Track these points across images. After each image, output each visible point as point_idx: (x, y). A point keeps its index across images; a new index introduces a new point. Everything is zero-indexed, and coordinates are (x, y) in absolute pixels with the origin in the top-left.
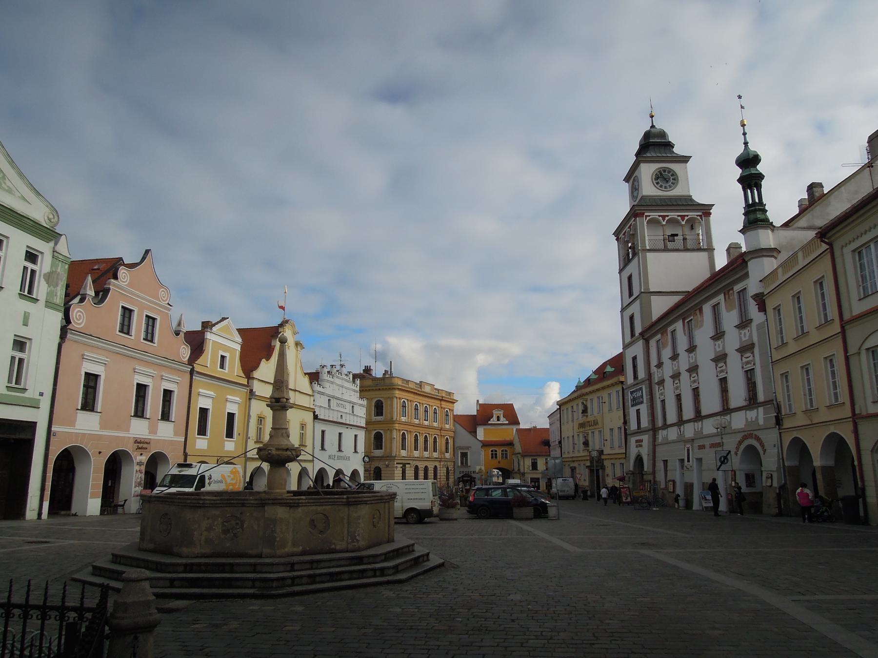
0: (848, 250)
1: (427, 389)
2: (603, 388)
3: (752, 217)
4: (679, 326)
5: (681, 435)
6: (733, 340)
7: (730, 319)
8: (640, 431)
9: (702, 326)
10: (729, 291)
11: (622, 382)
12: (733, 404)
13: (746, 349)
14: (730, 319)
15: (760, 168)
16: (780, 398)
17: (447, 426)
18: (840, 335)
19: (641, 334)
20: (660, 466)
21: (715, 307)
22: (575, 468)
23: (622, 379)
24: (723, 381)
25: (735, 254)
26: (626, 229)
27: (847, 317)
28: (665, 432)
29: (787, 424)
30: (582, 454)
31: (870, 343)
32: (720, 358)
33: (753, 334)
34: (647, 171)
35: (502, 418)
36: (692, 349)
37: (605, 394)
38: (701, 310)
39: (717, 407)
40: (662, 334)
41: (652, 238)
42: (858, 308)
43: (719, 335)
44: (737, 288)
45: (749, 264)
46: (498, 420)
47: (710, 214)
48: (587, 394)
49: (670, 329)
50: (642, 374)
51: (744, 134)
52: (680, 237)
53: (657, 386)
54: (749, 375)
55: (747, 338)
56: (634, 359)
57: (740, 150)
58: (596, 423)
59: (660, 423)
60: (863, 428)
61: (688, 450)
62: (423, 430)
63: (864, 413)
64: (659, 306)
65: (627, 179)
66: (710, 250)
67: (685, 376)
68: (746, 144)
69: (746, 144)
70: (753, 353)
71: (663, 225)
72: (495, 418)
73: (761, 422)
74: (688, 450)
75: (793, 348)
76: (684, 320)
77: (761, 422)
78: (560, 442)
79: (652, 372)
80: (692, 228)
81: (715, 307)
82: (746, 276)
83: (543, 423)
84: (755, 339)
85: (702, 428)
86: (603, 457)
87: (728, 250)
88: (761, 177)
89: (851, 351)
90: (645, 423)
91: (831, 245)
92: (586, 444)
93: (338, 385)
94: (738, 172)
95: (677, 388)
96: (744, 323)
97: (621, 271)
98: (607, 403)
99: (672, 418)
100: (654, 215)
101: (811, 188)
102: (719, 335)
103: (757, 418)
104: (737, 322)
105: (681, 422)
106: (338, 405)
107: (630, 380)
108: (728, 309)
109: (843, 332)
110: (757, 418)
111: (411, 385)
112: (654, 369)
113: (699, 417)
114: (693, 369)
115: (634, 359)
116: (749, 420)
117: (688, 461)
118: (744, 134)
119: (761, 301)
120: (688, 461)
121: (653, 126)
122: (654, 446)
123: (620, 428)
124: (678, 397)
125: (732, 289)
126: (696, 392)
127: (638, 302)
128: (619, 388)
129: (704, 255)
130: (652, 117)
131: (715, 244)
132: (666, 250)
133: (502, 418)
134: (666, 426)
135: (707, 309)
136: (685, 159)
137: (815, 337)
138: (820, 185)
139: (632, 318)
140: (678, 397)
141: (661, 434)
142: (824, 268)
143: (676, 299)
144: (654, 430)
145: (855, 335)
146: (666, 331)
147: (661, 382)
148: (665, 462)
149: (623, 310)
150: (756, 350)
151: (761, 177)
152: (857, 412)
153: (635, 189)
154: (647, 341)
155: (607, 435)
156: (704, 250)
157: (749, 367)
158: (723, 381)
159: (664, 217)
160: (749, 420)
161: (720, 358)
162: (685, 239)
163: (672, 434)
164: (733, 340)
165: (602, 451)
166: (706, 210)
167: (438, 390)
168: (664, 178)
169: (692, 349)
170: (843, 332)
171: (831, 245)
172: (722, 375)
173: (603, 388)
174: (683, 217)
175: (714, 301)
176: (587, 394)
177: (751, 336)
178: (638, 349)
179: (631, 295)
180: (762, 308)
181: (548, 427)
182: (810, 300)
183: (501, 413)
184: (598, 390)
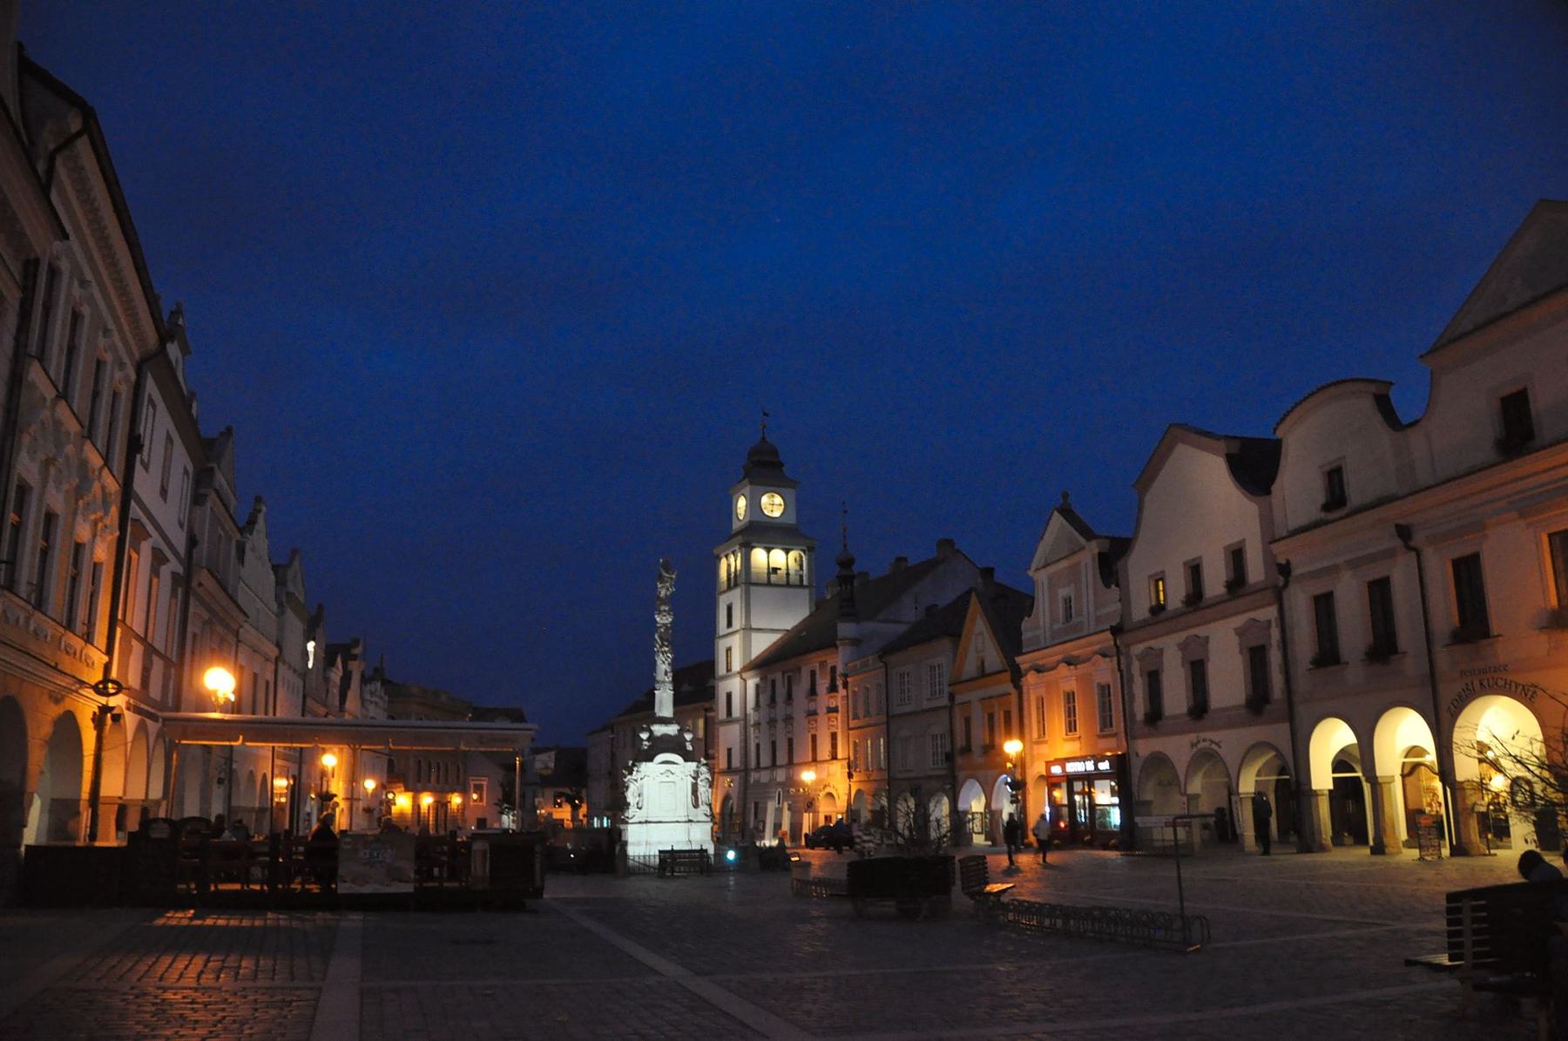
4: (778, 676)
5: (773, 780)
7: (823, 684)
8: (730, 770)
14: (823, 684)
19: (740, 673)
21: (813, 674)
23: (707, 705)
42: (897, 710)
49: (770, 677)
50: (736, 712)
59: (753, 764)
67: (780, 725)
81: (813, 674)
90: (736, 763)
99: (765, 760)
105: (774, 765)
107: (722, 714)
112: (750, 710)
114: (789, 719)
124: (774, 744)
126: (790, 741)
132: (769, 584)
134: (758, 768)
140: (774, 744)
141: (753, 776)
143: (775, 637)
144: (745, 771)
148: (756, 804)
163: (764, 777)
179: (730, 624)
180: (845, 686)
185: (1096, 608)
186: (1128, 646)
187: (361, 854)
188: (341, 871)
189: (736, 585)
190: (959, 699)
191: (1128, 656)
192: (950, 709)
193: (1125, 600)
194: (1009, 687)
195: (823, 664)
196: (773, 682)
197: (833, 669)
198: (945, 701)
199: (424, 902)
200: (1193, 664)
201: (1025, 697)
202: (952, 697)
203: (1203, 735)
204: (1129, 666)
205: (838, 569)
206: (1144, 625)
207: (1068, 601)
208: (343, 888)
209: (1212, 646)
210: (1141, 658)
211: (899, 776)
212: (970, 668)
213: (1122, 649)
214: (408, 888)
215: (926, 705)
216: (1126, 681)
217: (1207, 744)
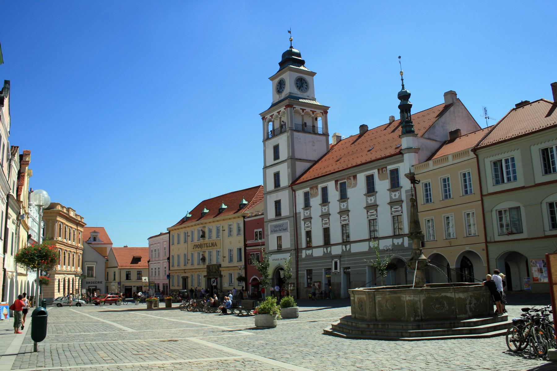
1: (72, 214)
7: (382, 185)
9: (355, 185)
10: (382, 169)
12: (380, 234)
14: (382, 185)
15: (411, 101)
17: (80, 245)
18: (480, 202)
20: (303, 273)
22: (187, 277)
26: (275, 113)
27: (485, 193)
28: (309, 252)
29: (427, 245)
30: (196, 266)
34: (289, 77)
38: (355, 177)
40: (311, 188)
45: (405, 155)
47: (327, 112)
48: (206, 223)
51: (402, 80)
53: (302, 222)
55: (397, 197)
56: (278, 204)
57: (400, 89)
58: (213, 245)
59: (304, 245)
60: (491, 247)
61: (336, 263)
62: (69, 249)
63: (493, 240)
65: (272, 78)
66: (326, 134)
68: (403, 85)
69: (403, 85)
70: (401, 206)
71: (302, 116)
73: (406, 244)
74: (336, 263)
76: (336, 182)
77: (406, 244)
78: (169, 259)
79: (298, 211)
82: (402, 161)
83: (146, 245)
85: (350, 249)
86: (221, 269)
88: (410, 106)
92: (203, 259)
94: (399, 102)
95: (326, 224)
97: (264, 141)
103: (403, 243)
108: (380, 179)
110: (403, 243)
111: (65, 210)
113: (346, 241)
114: (344, 212)
115: (278, 204)
116: (396, 244)
117: (336, 268)
118: (402, 80)
120: (336, 268)
121: (291, 47)
122: (297, 262)
123: (240, 249)
125: (386, 168)
127: (285, 165)
130: (291, 41)
136: (313, 74)
139: (277, 176)
147: (308, 219)
149: (265, 168)
150: (404, 205)
151: (410, 106)
152: (488, 240)
153: (280, 87)
154: (294, 191)
155: (227, 254)
159: (303, 110)
160: (396, 244)
165: (220, 265)
166: (325, 110)
167: (76, 215)
168: (302, 83)
170: (482, 200)
176: (206, 223)
177: (400, 196)
178: (284, 197)
181: (147, 246)
189: (281, 132)
195: (381, 170)
196: (325, 190)
205: (400, 101)
211: (497, 238)
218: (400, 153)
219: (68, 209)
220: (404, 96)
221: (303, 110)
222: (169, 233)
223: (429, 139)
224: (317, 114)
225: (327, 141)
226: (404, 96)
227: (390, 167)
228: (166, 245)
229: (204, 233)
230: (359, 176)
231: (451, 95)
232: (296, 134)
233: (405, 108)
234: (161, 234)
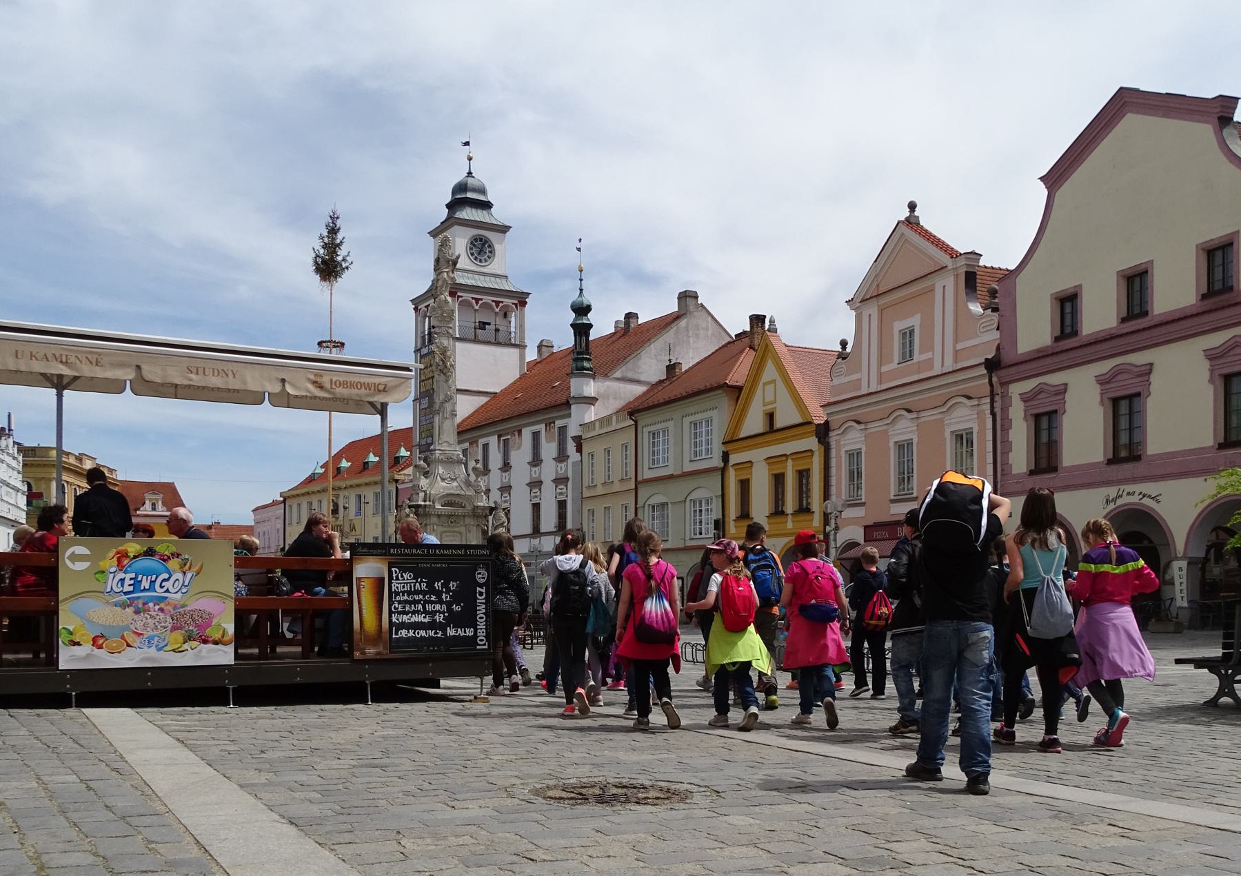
0: (646, 430)
2: (367, 484)
3: (579, 364)
4: (493, 441)
6: (549, 470)
7: (549, 450)
9: (519, 448)
11: (397, 481)
13: (560, 481)
14: (549, 450)
16: (585, 529)
21: (536, 435)
24: (536, 507)
25: (545, 355)
27: (640, 479)
31: (651, 501)
32: (536, 484)
33: (568, 469)
35: (160, 506)
36: (506, 467)
37: (369, 494)
38: (520, 432)
39: (529, 530)
41: (464, 324)
42: (648, 474)
43: (536, 461)
44: (559, 423)
46: (154, 509)
49: (482, 441)
52: (492, 327)
54: (562, 505)
64: (465, 407)
66: (522, 346)
72: (148, 505)
75: (600, 490)
76: (499, 437)
80: (505, 315)
81: (536, 435)
82: (569, 416)
84: (570, 475)
87: (540, 347)
88: (590, 326)
89: (640, 504)
91: (636, 422)
93: (8, 465)
96: (562, 457)
98: (371, 503)
100: (467, 296)
101: (629, 316)
102: (536, 461)
104: (555, 455)
106: (8, 493)
109: (636, 489)
119: (578, 441)
128: (392, 488)
129: (516, 351)
131: (527, 342)
132: (476, 340)
133: (160, 506)
135: (527, 433)
137: (617, 487)
138: (636, 316)
142: (629, 437)
143: (483, 400)
145: (643, 493)
146: (477, 442)
150: (570, 484)
151: (590, 326)
156: (515, 346)
157: (562, 498)
158: (536, 507)
159: (477, 300)
161: (536, 484)
162: (497, 330)
164: (549, 470)
166: (521, 299)
169: (506, 467)
170: (636, 489)
171: (636, 422)
172: (536, 501)
173: (367, 484)
174: (497, 303)
175: (535, 428)
180: (579, 449)
182: (617, 455)
183: (160, 497)
184: (358, 486)
185: (956, 341)
186: (1004, 384)
187: (112, 583)
188: (67, 620)
190: (733, 459)
191: (1006, 398)
192: (723, 471)
193: (1007, 327)
194: (812, 443)
196: (486, 446)
197: (563, 430)
198: (717, 462)
199: (248, 686)
200: (1037, 417)
201: (833, 453)
202: (725, 457)
203: (1129, 488)
204: (1005, 410)
206: (1039, 356)
207: (908, 335)
208: (68, 659)
209: (1155, 378)
210: (1026, 398)
212: (754, 423)
213: (998, 389)
214: (224, 656)
215: (689, 467)
216: (1000, 426)
217: (1135, 499)
218: (567, 404)
219: (80, 458)
220: (582, 310)
221: (477, 300)
222: (284, 502)
223: (624, 379)
224: (507, 306)
225: (522, 356)
226: (582, 310)
227: (559, 423)
228: (280, 525)
229: (336, 506)
230: (524, 431)
231: (687, 298)
232: (459, 345)
233: (581, 330)
234: (275, 503)
